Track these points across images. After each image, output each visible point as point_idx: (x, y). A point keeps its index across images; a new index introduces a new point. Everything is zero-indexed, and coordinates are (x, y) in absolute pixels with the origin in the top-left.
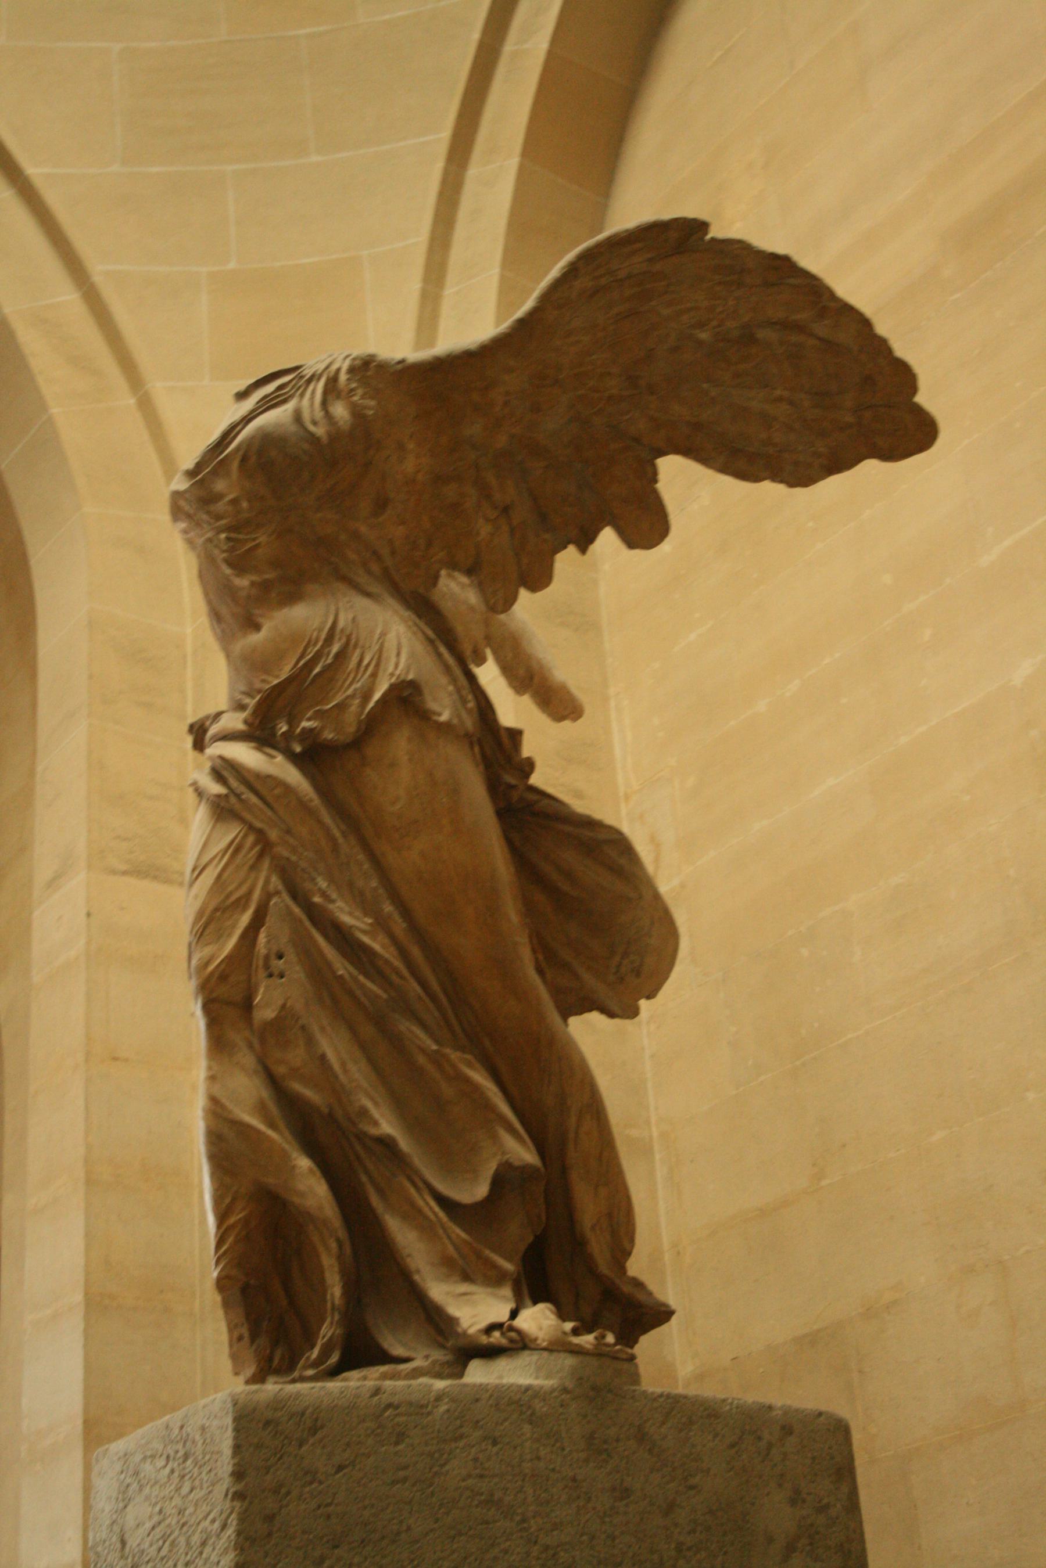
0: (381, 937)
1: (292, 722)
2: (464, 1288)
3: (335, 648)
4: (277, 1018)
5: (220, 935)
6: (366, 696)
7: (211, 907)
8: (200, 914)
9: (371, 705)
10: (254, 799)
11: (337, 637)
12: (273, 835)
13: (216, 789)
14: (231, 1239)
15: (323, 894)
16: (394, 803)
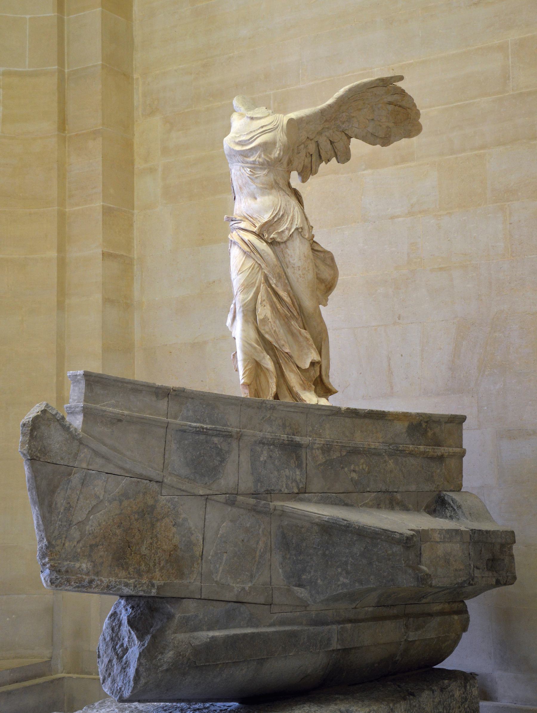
0: (289, 298)
1: (269, 234)
2: (304, 392)
3: (281, 213)
4: (263, 319)
5: (247, 293)
6: (290, 230)
7: (246, 283)
8: (243, 285)
9: (291, 233)
10: (258, 256)
11: (282, 208)
12: (263, 266)
13: (246, 249)
14: (247, 373)
15: (275, 284)
16: (294, 260)
